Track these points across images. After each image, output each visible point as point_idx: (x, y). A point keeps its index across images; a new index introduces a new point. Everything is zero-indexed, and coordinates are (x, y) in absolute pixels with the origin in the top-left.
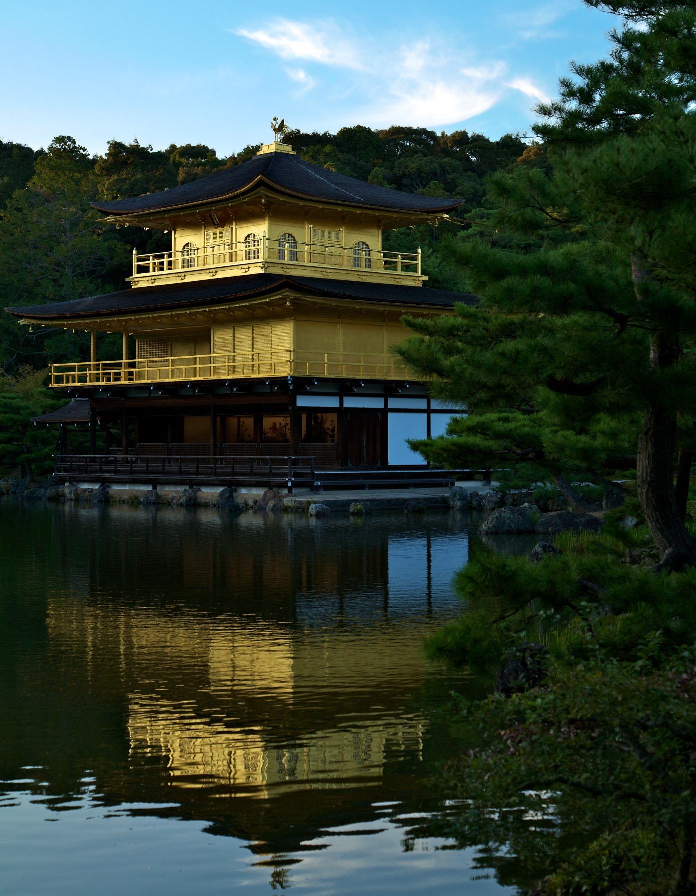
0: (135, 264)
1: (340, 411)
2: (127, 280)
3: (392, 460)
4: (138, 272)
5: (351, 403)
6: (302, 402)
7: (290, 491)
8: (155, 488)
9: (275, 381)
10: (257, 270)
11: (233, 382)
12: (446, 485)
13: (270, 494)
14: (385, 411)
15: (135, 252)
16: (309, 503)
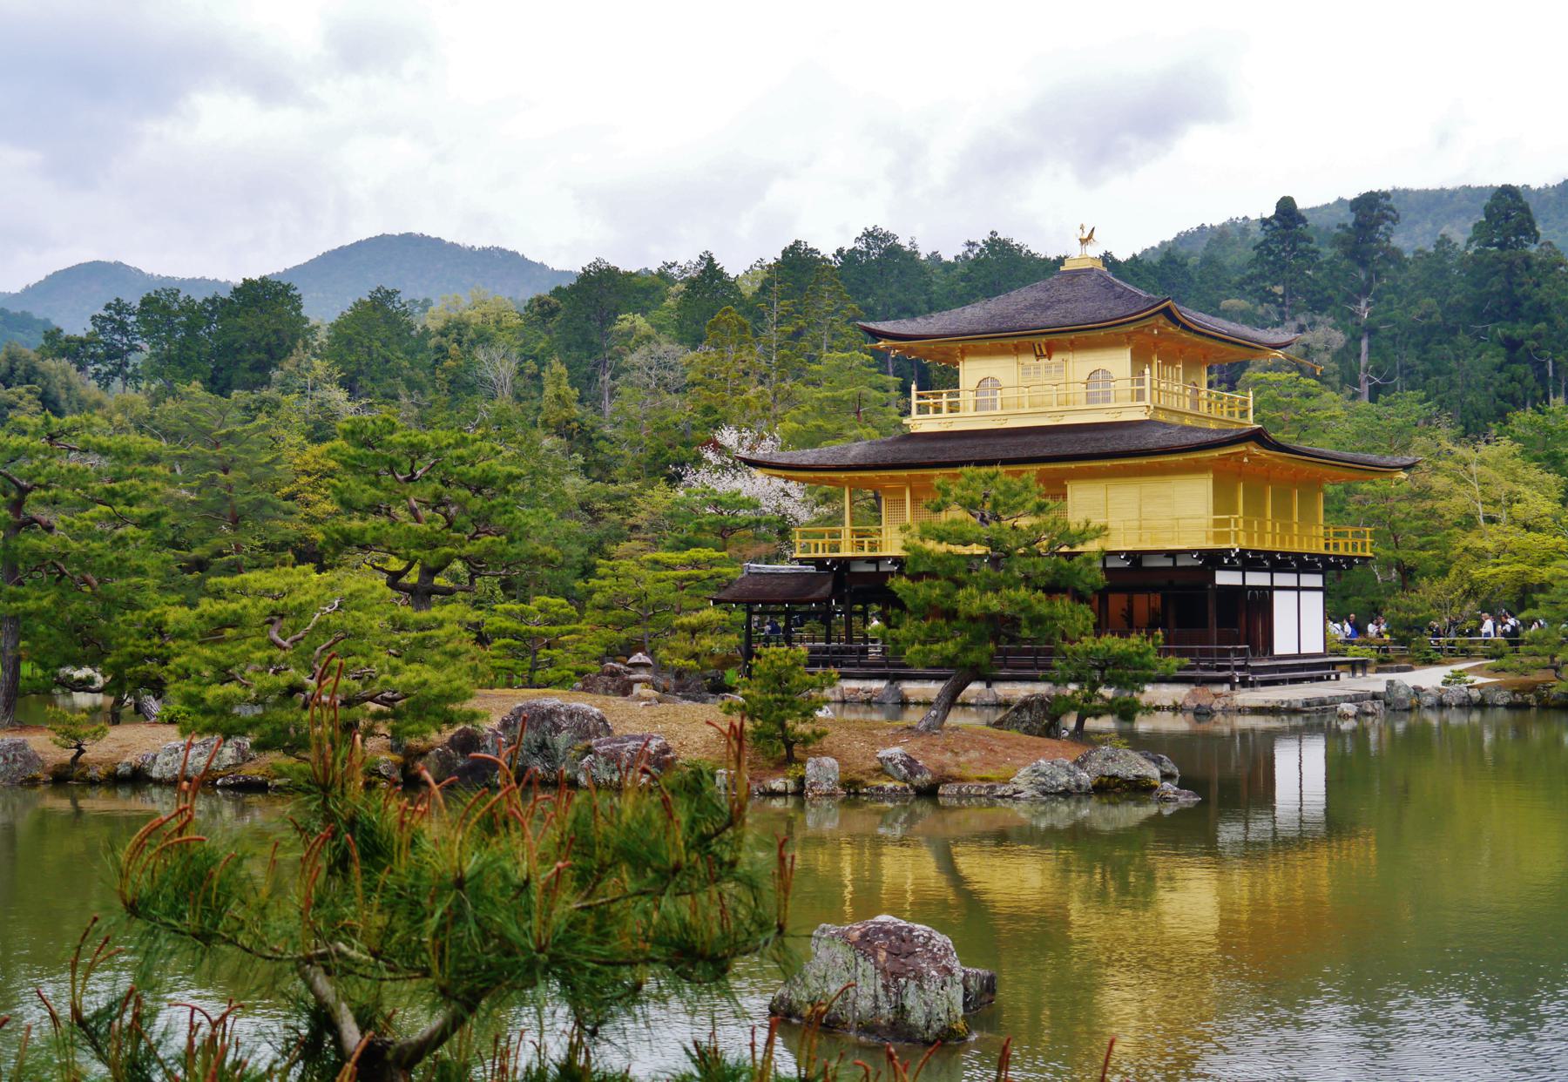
0: (914, 401)
1: (1243, 589)
2: (906, 421)
3: (1277, 652)
4: (919, 412)
5: (1257, 579)
6: (1224, 578)
7: (1232, 688)
8: (989, 686)
9: (1203, 553)
10: (1142, 417)
11: (1130, 555)
12: (1329, 678)
13: (1199, 690)
14: (1272, 588)
15: (914, 387)
16: (1335, 700)
